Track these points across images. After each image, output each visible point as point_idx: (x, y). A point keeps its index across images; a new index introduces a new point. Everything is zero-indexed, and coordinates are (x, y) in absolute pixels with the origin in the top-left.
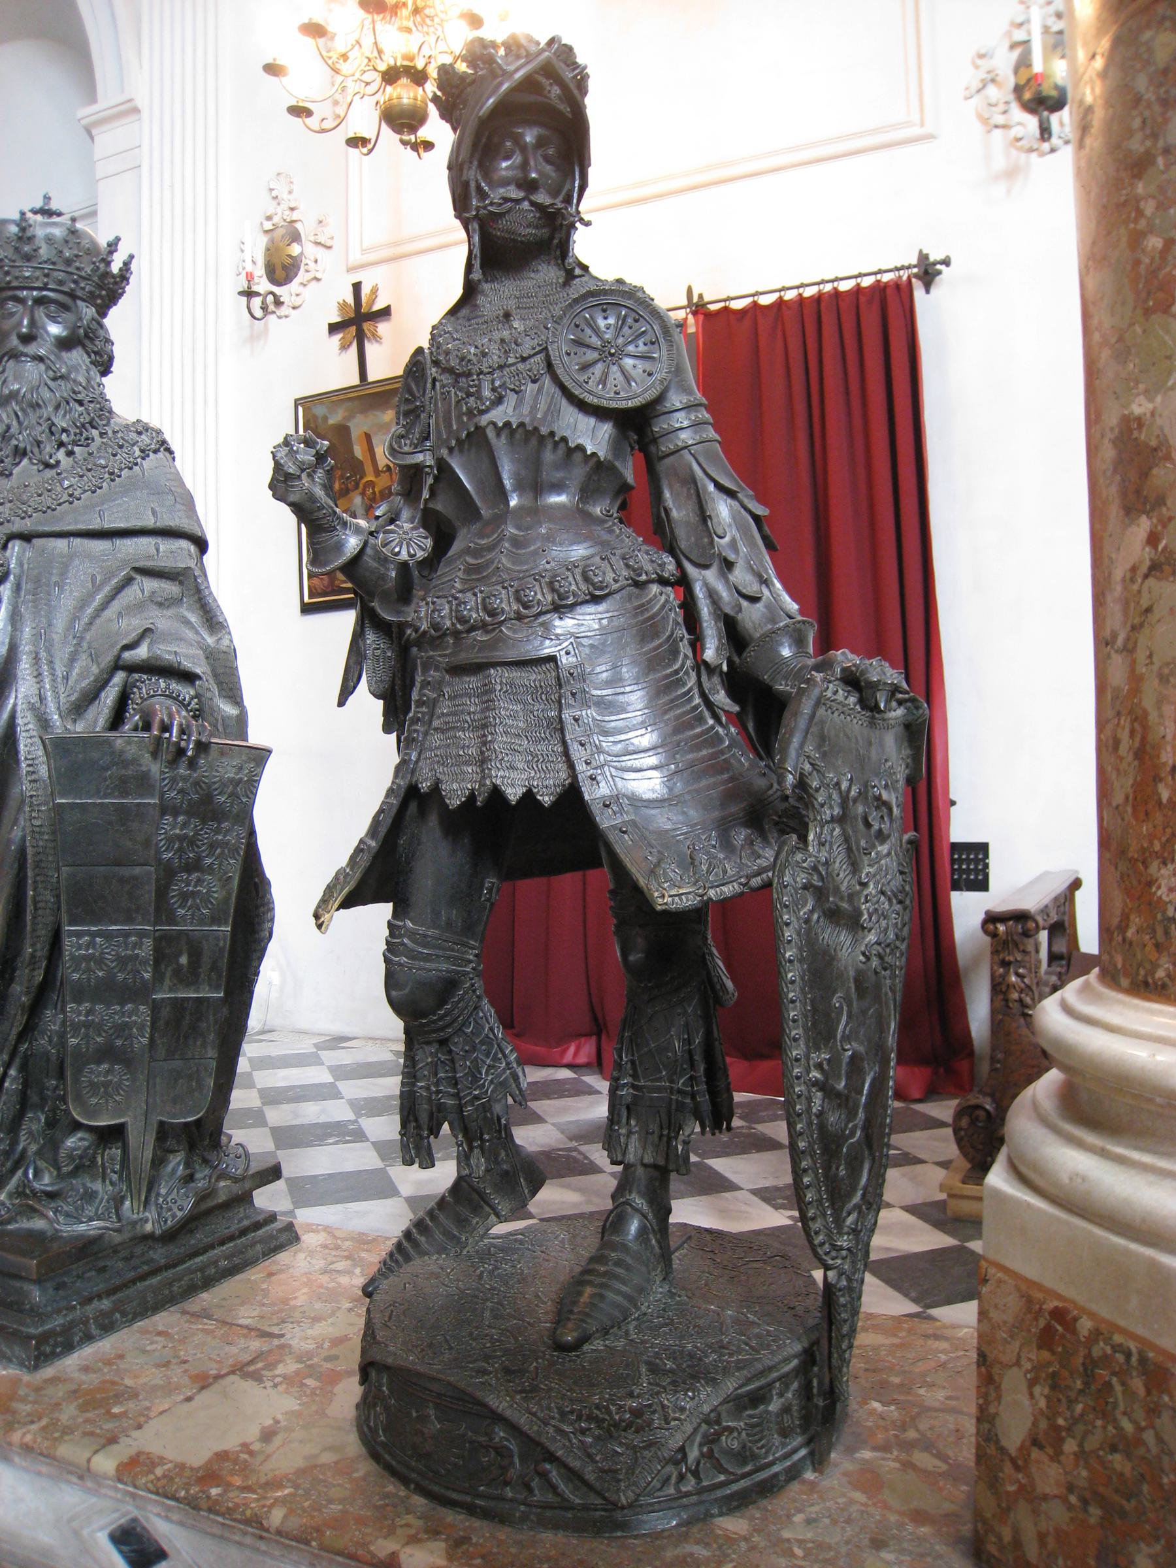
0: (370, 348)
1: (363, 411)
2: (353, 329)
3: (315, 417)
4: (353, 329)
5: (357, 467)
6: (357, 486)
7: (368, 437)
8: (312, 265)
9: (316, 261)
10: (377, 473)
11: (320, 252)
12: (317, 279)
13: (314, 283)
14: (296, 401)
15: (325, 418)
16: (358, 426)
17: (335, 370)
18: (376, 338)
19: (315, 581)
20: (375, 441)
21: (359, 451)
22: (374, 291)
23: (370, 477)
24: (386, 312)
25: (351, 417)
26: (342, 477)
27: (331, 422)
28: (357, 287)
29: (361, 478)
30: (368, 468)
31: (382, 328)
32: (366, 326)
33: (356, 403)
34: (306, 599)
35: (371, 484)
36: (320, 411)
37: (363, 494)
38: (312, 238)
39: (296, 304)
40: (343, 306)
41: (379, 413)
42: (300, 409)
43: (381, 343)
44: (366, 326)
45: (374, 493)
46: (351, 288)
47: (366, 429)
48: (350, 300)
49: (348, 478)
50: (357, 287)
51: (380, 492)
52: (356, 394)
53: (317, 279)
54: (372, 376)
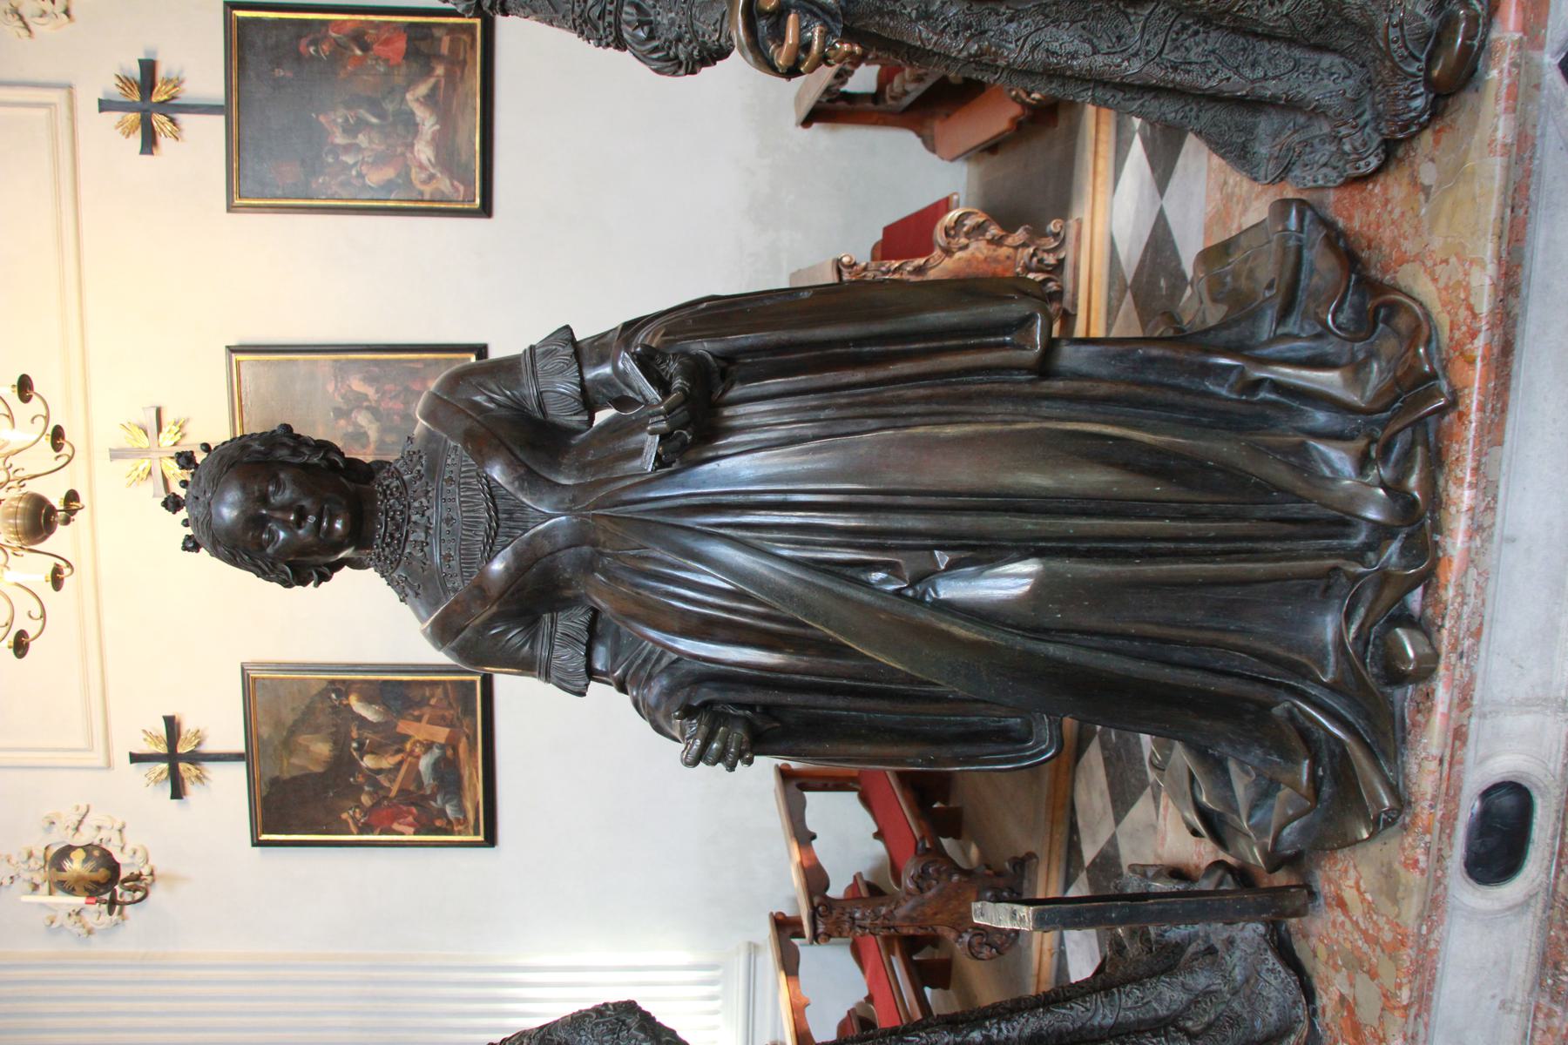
0: (209, 747)
9: (99, 828)
11: (91, 820)
13: (126, 832)
14: (254, 845)
17: (226, 794)
18: (199, 738)
24: (171, 724)
28: (135, 758)
31: (187, 727)
32: (182, 749)
34: (480, 838)
38: (71, 832)
50: (135, 758)
54: (240, 747)
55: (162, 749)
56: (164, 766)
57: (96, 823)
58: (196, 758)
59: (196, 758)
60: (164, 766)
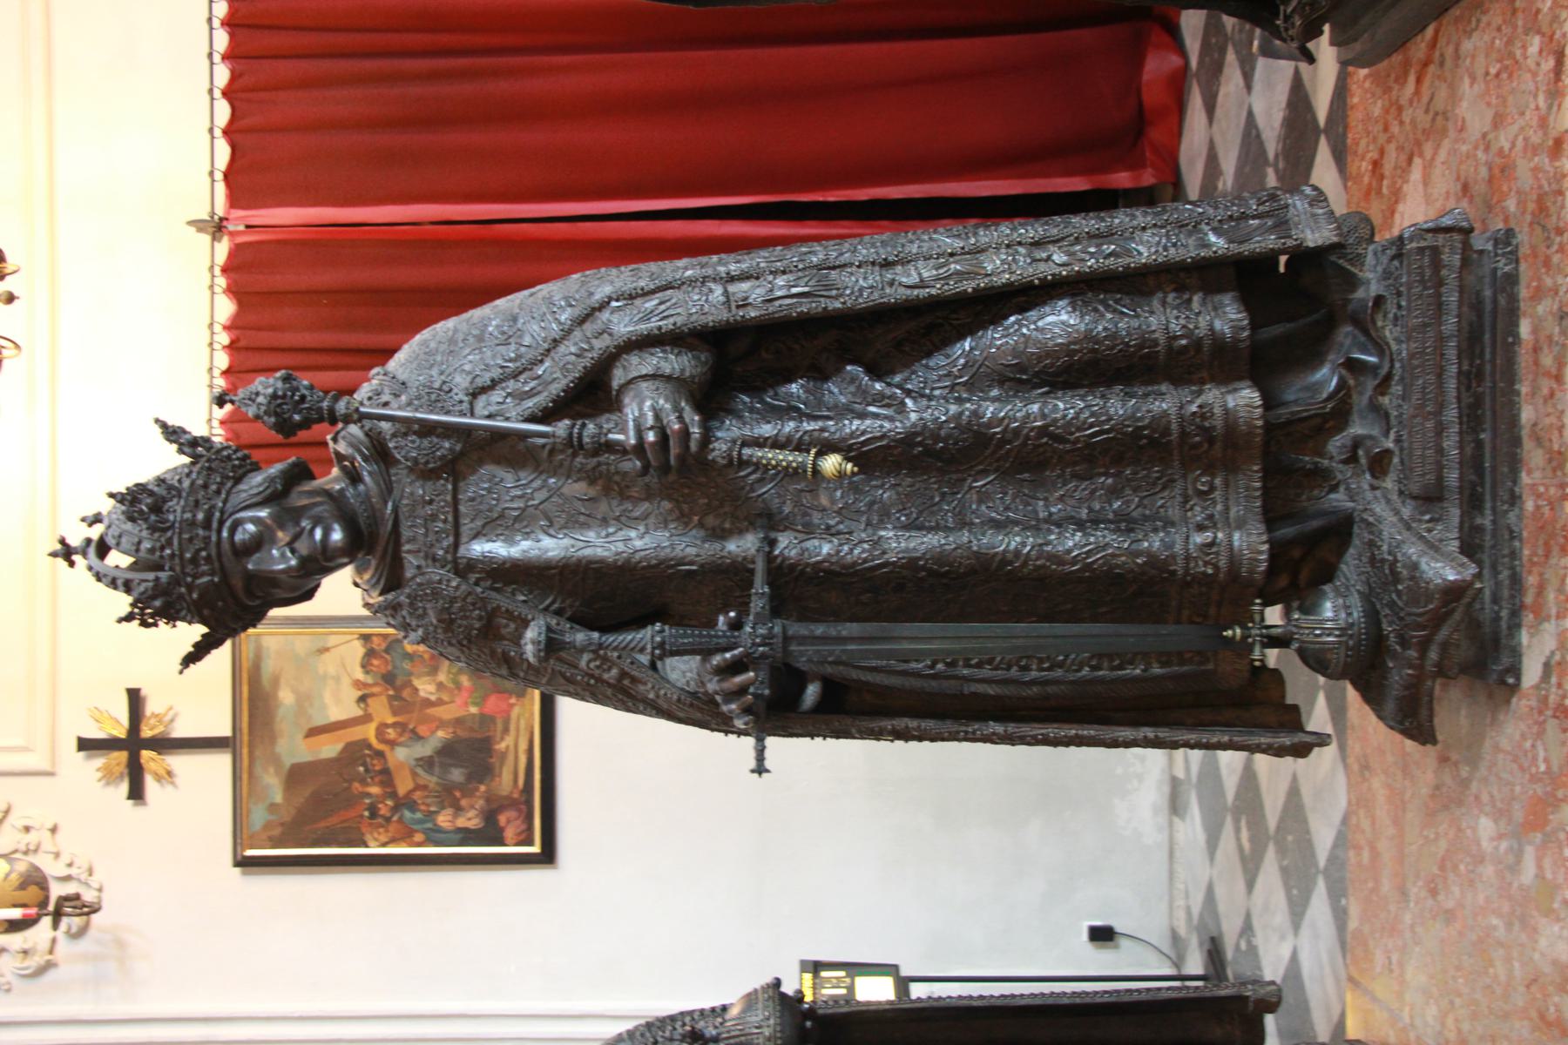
0: (179, 731)
1: (273, 739)
2: (146, 754)
3: (267, 826)
4: (146, 754)
5: (355, 753)
6: (380, 755)
7: (314, 732)
8: (32, 838)
9: (27, 829)
10: (366, 719)
11: (15, 820)
12: (54, 830)
13: (60, 836)
15: (273, 807)
16: (294, 748)
17: (200, 791)
19: (509, 833)
20: (319, 721)
21: (329, 749)
22: (98, 716)
23: (369, 732)
24: (135, 698)
25: (276, 760)
26: (363, 782)
27: (278, 798)
28: (85, 745)
29: (370, 746)
30: (356, 733)
31: (152, 707)
32: (146, 732)
33: (258, 753)
34: (535, 849)
35: (382, 728)
36: (258, 817)
37: (392, 744)
39: (86, 866)
40: (109, 777)
41: (281, 712)
42: (249, 853)
43: (176, 715)
44: (146, 732)
45: (394, 725)
46: (82, 754)
47: (300, 736)
48: (99, 761)
49: (367, 770)
51: (395, 713)
52: (245, 751)
53: (54, 830)
55: (121, 732)
56: (122, 756)
57: (21, 823)
58: (166, 744)
59: (166, 744)
60: (122, 756)
